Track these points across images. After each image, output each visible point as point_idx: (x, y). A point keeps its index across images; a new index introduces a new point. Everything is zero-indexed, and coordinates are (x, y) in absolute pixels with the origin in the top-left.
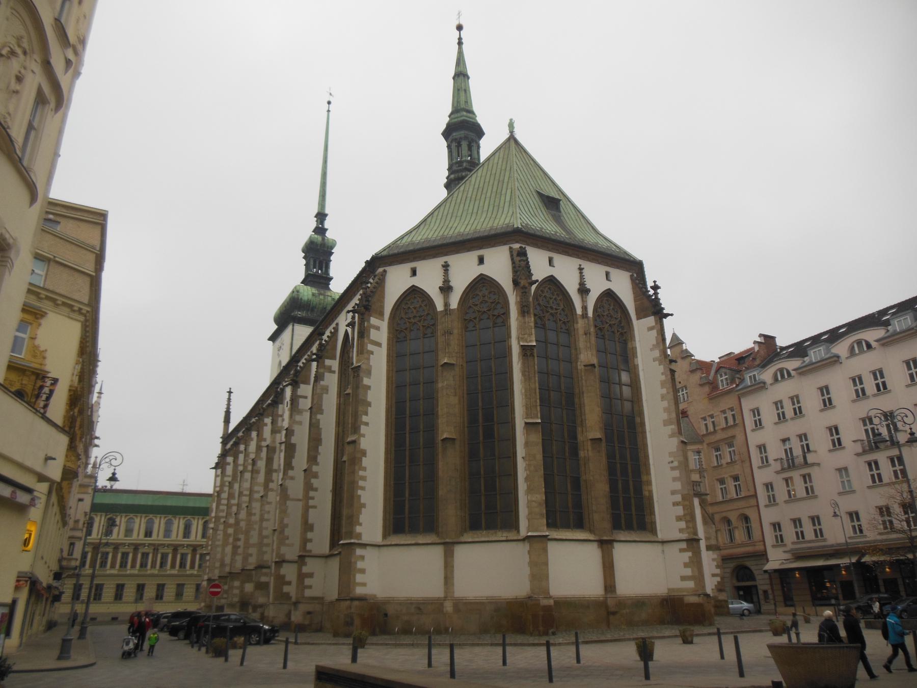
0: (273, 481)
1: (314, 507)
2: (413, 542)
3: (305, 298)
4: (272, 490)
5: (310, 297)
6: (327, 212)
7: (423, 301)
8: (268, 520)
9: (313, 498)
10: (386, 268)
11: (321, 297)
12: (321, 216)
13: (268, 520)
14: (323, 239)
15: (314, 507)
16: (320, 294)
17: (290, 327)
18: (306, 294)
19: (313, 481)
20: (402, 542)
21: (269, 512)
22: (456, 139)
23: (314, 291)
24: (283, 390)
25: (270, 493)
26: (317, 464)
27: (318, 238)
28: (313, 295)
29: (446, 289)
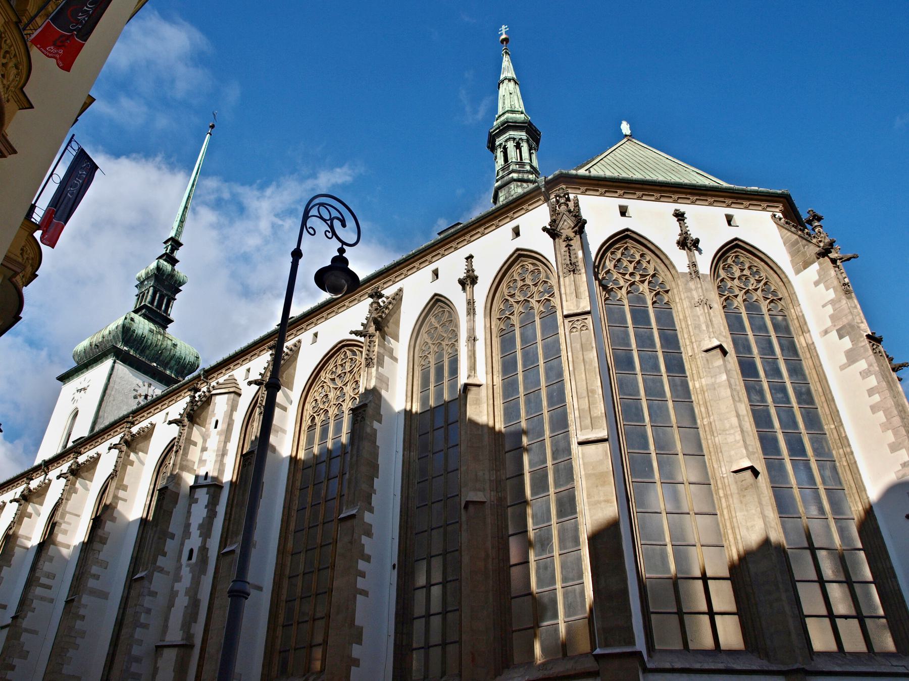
0: (164, 554)
1: (365, 593)
2: (721, 666)
3: (140, 332)
4: (161, 570)
5: (146, 332)
6: (181, 240)
7: (642, 255)
8: (145, 626)
9: (363, 575)
10: (579, 197)
11: (159, 337)
12: (175, 244)
13: (145, 626)
14: (173, 270)
15: (365, 593)
16: (159, 333)
17: (108, 363)
18: (141, 326)
19: (364, 539)
20: (697, 666)
21: (148, 611)
22: (514, 139)
23: (152, 326)
24: (208, 400)
25: (156, 574)
26: (371, 510)
27: (168, 267)
28: (151, 331)
29: (687, 243)
